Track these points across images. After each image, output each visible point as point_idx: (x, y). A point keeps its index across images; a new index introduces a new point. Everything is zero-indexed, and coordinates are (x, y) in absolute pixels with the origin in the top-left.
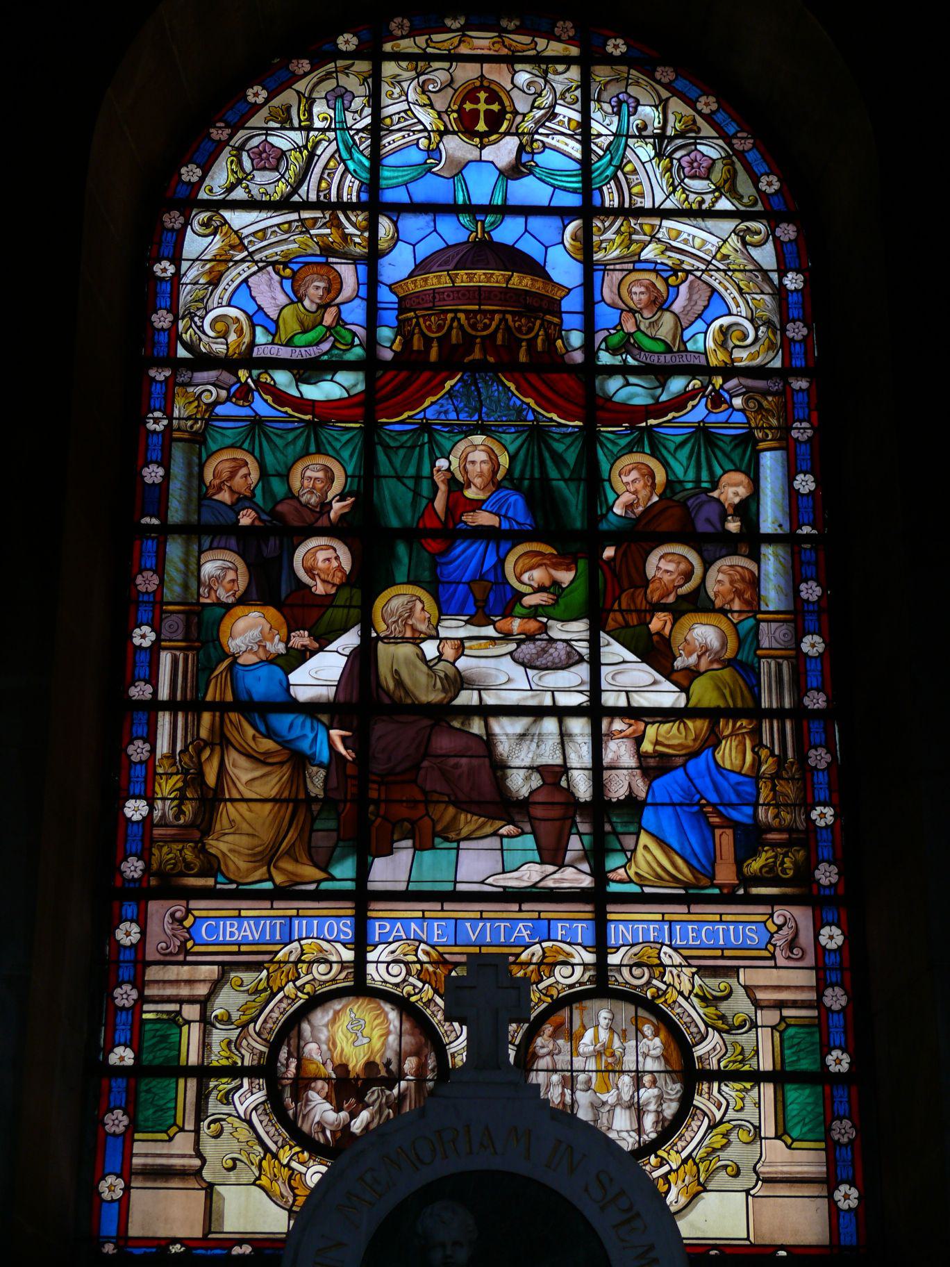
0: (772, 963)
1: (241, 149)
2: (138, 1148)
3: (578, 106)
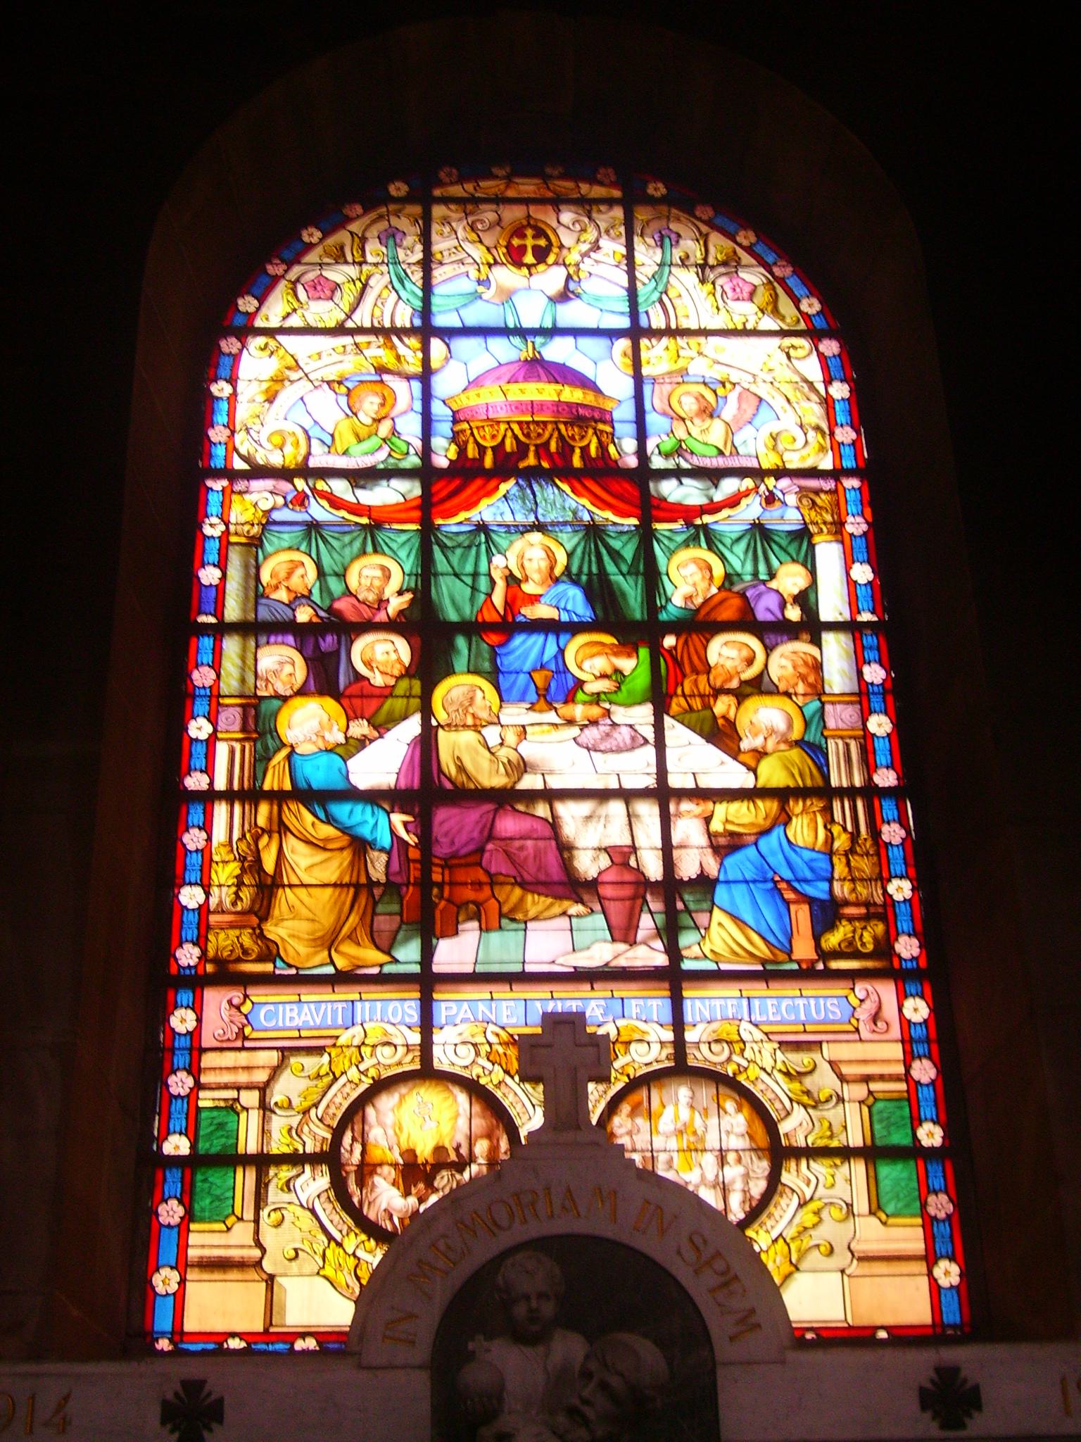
0: (856, 1037)
1: (295, 283)
2: (193, 1239)
3: (623, 240)
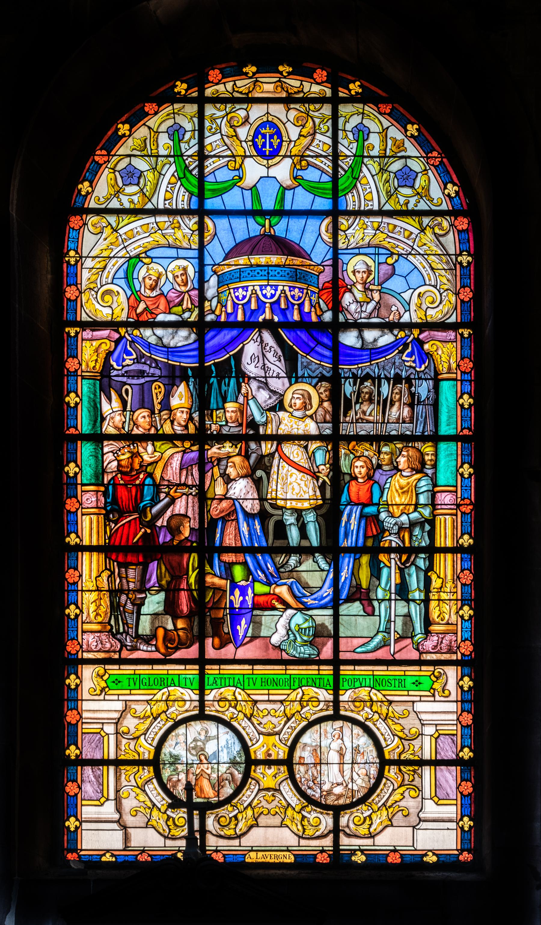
0: (432, 699)
3: (329, 134)
